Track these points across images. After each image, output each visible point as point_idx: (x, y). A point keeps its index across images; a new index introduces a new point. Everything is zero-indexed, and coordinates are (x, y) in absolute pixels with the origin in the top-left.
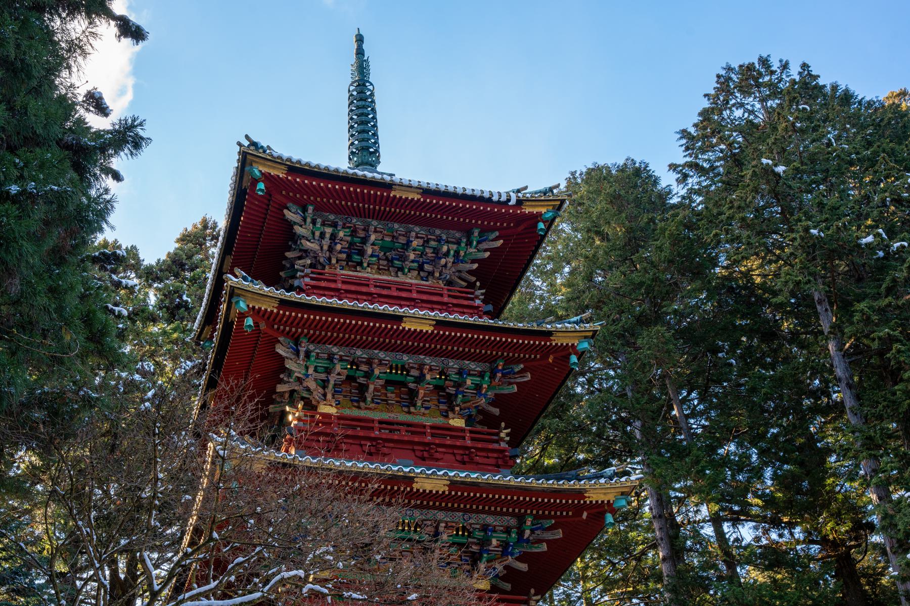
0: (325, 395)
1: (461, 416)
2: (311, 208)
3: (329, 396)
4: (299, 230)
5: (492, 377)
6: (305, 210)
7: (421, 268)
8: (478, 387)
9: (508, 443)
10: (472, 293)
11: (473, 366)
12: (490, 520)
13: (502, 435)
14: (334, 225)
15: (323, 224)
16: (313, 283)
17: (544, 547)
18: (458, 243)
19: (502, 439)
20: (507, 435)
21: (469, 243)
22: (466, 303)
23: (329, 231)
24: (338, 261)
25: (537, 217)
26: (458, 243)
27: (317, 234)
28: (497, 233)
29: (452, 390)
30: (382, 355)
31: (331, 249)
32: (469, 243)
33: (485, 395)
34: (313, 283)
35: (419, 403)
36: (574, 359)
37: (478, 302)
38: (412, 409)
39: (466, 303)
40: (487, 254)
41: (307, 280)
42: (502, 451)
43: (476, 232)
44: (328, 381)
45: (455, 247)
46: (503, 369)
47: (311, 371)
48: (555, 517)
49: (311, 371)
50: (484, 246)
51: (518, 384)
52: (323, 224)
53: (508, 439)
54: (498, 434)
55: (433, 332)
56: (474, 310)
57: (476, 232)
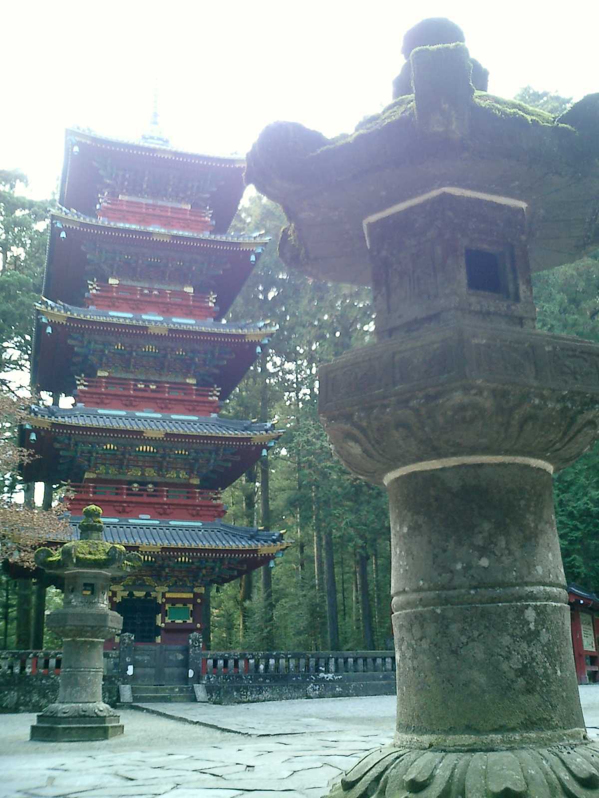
0: (112, 273)
1: (191, 285)
3: (114, 273)
4: (101, 172)
9: (214, 303)
10: (205, 213)
13: (211, 299)
16: (109, 206)
17: (225, 362)
20: (216, 298)
22: (199, 219)
34: (109, 206)
36: (253, 258)
42: (210, 308)
53: (214, 301)
54: (209, 298)
55: (170, 241)
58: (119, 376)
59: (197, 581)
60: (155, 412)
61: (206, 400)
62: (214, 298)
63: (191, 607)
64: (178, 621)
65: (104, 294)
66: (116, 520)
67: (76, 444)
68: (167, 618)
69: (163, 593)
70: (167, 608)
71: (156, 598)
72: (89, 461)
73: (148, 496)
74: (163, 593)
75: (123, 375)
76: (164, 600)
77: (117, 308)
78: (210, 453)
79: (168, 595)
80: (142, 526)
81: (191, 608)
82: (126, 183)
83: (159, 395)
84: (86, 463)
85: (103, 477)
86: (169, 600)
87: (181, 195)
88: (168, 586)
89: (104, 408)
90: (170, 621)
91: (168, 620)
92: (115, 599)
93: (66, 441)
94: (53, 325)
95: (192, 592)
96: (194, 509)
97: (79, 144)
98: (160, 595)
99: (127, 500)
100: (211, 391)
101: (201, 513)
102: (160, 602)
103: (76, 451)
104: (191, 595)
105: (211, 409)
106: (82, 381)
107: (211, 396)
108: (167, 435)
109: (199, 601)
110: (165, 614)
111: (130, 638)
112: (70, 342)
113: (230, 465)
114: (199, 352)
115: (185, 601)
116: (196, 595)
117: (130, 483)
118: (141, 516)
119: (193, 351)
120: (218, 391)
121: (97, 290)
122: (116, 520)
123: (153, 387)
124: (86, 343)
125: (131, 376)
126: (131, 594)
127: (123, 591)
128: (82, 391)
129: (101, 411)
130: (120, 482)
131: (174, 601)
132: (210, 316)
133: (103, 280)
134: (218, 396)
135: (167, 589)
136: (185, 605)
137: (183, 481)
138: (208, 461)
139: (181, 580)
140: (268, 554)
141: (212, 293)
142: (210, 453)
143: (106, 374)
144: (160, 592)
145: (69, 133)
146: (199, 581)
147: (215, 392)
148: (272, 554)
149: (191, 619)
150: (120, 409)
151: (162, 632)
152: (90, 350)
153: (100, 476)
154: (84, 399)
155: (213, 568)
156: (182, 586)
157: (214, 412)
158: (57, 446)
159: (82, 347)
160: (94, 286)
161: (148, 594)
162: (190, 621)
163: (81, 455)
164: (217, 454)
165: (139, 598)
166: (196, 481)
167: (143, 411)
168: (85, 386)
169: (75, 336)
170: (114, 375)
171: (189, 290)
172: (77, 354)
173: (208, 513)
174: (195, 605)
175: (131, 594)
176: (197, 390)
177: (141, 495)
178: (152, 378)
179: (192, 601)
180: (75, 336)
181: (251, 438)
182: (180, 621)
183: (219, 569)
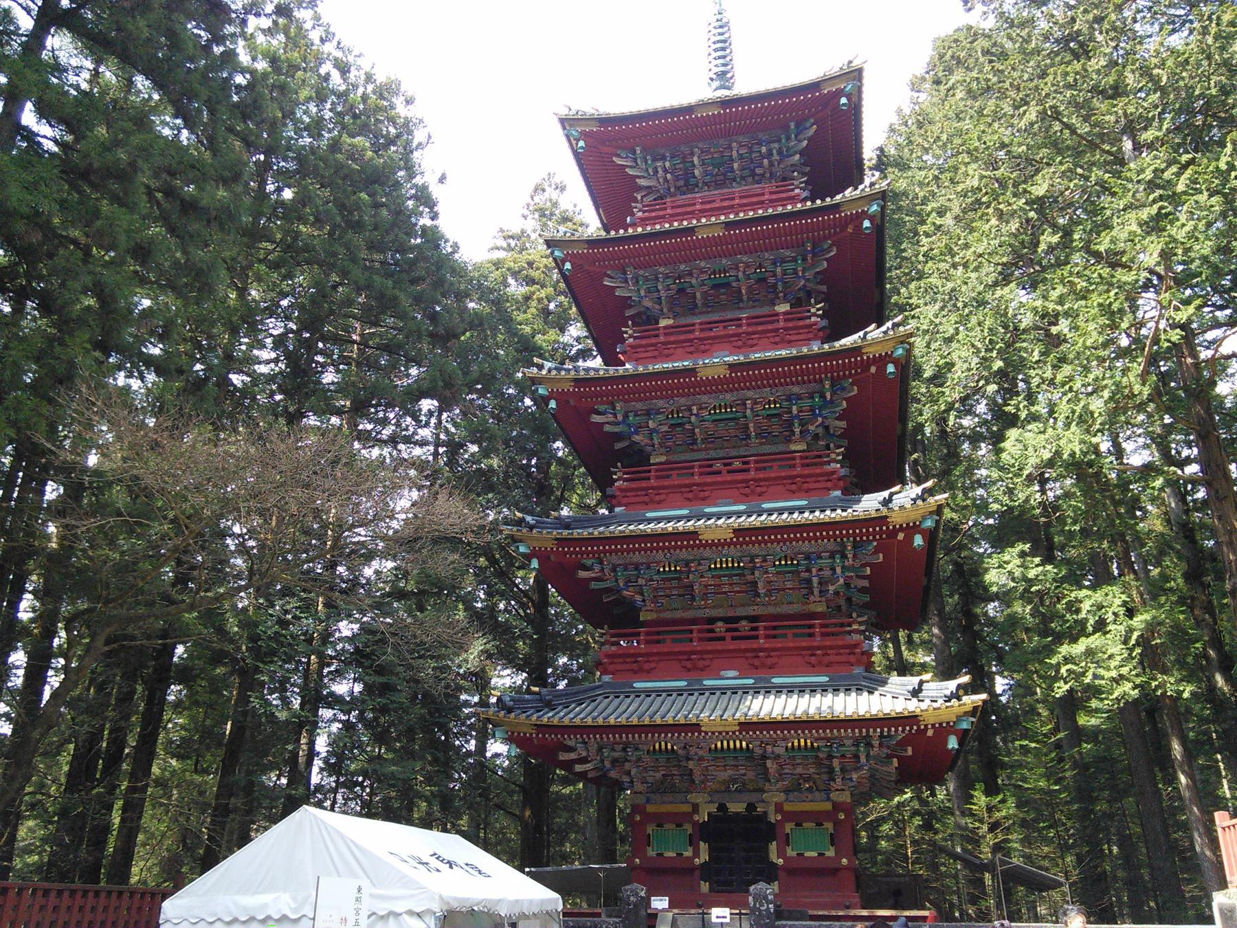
1: (785, 300)
2: (638, 150)
3: (665, 310)
4: (630, 172)
5: (804, 259)
6: (634, 152)
7: (753, 174)
8: (795, 272)
11: (788, 253)
12: (796, 389)
14: (664, 158)
15: (654, 160)
18: (779, 141)
19: (814, 315)
21: (788, 138)
22: (784, 195)
23: (659, 164)
24: (677, 188)
25: (840, 93)
26: (779, 141)
27: (650, 170)
28: (812, 120)
29: (771, 280)
30: (703, 264)
31: (666, 180)
32: (788, 138)
33: (804, 277)
35: (745, 298)
37: (797, 191)
38: (741, 305)
39: (784, 195)
40: (805, 143)
41: (640, 214)
42: (815, 324)
43: (792, 125)
44: (660, 298)
45: (776, 145)
46: (814, 248)
47: (642, 293)
48: (850, 375)
49: (642, 293)
50: (801, 136)
51: (827, 260)
52: (654, 160)
56: (793, 200)
57: (792, 125)
58: (683, 458)
59: (834, 780)
60: (734, 503)
61: (818, 471)
62: (818, 310)
63: (829, 826)
64: (808, 854)
65: (644, 342)
66: (683, 684)
67: (614, 570)
68: (789, 850)
69: (776, 804)
70: (788, 830)
71: (765, 813)
72: (642, 594)
73: (733, 638)
74: (776, 804)
75: (689, 456)
76: (779, 818)
77: (668, 357)
78: (832, 557)
79: (787, 807)
80: (723, 690)
81: (831, 830)
82: (669, 176)
83: (740, 476)
84: (638, 598)
85: (668, 615)
86: (788, 816)
87: (758, 171)
88: (787, 791)
89: (655, 510)
90: (794, 854)
91: (791, 852)
92: (696, 818)
93: (597, 568)
94: (560, 397)
95: (828, 799)
96: (814, 655)
97: (585, 135)
98: (772, 808)
99: (699, 648)
100: (828, 456)
101: (827, 659)
102: (773, 821)
103: (617, 580)
104: (828, 806)
105: (829, 484)
106: (619, 474)
107: (829, 463)
108: (738, 532)
109: (842, 816)
110: (787, 840)
111: (637, 894)
112: (596, 418)
113: (868, 571)
114: (799, 397)
115: (819, 818)
116: (837, 807)
117: (712, 620)
118: (723, 673)
119: (789, 399)
120: (838, 454)
121: (635, 338)
122: (683, 684)
123: (737, 464)
124: (620, 418)
125: (702, 455)
126: (722, 807)
127: (710, 802)
128: (620, 489)
129: (649, 515)
130: (694, 621)
131: (799, 818)
132: (815, 338)
133: (646, 320)
134: (837, 462)
135: (783, 796)
136: (819, 824)
137: (796, 608)
138: (833, 569)
139: (806, 781)
140: (941, 724)
141: (813, 301)
142: (832, 557)
143: (663, 459)
144: (772, 802)
145: (563, 121)
146: (839, 780)
147: (833, 456)
148: (948, 723)
149: (832, 849)
150: (680, 508)
151: (782, 874)
152: (629, 426)
153: (661, 615)
154: (625, 501)
155: (856, 757)
156: (810, 790)
157: (836, 488)
158: (582, 574)
159: (618, 424)
160: (630, 332)
161: (751, 807)
162: (830, 853)
163: (626, 584)
164: (844, 556)
165: (737, 814)
166: (820, 608)
167: (716, 505)
168: (625, 480)
169: (602, 408)
170: (676, 458)
171: (783, 308)
172: (618, 437)
173: (839, 658)
174: (837, 823)
175: (722, 807)
176: (802, 458)
177: (723, 639)
178: (734, 453)
179: (830, 815)
180: (602, 408)
181: (886, 517)
182: (815, 854)
183: (868, 756)
